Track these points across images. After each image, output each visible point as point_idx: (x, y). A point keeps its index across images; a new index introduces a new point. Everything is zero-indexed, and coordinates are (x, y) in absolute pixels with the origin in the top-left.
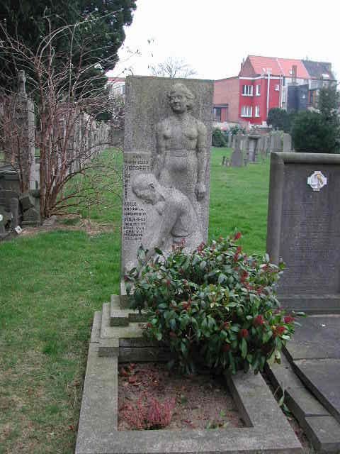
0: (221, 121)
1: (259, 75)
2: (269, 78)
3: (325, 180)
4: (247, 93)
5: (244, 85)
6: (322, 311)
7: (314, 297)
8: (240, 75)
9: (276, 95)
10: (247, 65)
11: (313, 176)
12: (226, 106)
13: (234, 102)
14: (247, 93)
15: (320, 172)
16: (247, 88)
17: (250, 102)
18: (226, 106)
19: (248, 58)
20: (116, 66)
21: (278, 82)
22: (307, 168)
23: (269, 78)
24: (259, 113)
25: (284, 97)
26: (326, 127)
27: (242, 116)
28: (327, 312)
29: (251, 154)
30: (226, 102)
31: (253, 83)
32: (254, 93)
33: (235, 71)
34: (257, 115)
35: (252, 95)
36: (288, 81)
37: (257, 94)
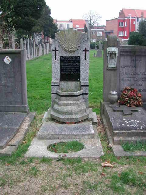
1: (126, 17)
2: (131, 18)
3: (10, 60)
4: (122, 25)
5: (120, 22)
6: (19, 111)
7: (11, 106)
8: (118, 18)
9: (134, 26)
10: (122, 13)
11: (5, 58)
13: (116, 30)
14: (121, 25)
15: (8, 57)
16: (121, 23)
17: (123, 29)
19: (122, 10)
20: (52, 18)
21: (134, 20)
22: (3, 56)
23: (131, 18)
24: (126, 34)
25: (137, 26)
26: (142, 39)
28: (15, 112)
30: (112, 30)
31: (124, 21)
32: (124, 25)
33: (116, 15)
34: (126, 35)
35: (123, 26)
36: (140, 19)
37: (126, 26)
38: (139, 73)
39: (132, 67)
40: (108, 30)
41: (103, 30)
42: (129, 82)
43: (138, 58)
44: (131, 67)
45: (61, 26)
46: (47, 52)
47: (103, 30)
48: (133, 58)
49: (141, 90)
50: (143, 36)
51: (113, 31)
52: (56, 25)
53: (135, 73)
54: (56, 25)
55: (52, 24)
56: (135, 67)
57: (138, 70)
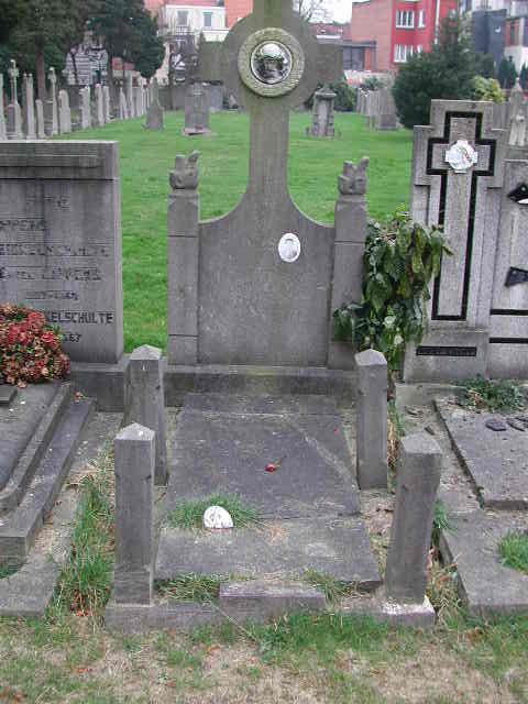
0: (363, 68)
4: (404, 24)
12: (372, 45)
13: (384, 41)
14: (404, 24)
16: (405, 14)
18: (372, 45)
27: (396, 61)
29: (322, 123)
37: (421, 25)
38: (61, 251)
39: (32, 226)
40: (359, 38)
41: (338, 37)
42: (28, 285)
43: (52, 191)
44: (28, 225)
45: (183, 17)
46: (101, 119)
47: (338, 37)
48: (34, 191)
49: (76, 318)
50: (450, 67)
51: (375, 43)
52: (152, 19)
53: (45, 250)
54: (153, 15)
55: (138, 11)
56: (43, 223)
57: (56, 237)
